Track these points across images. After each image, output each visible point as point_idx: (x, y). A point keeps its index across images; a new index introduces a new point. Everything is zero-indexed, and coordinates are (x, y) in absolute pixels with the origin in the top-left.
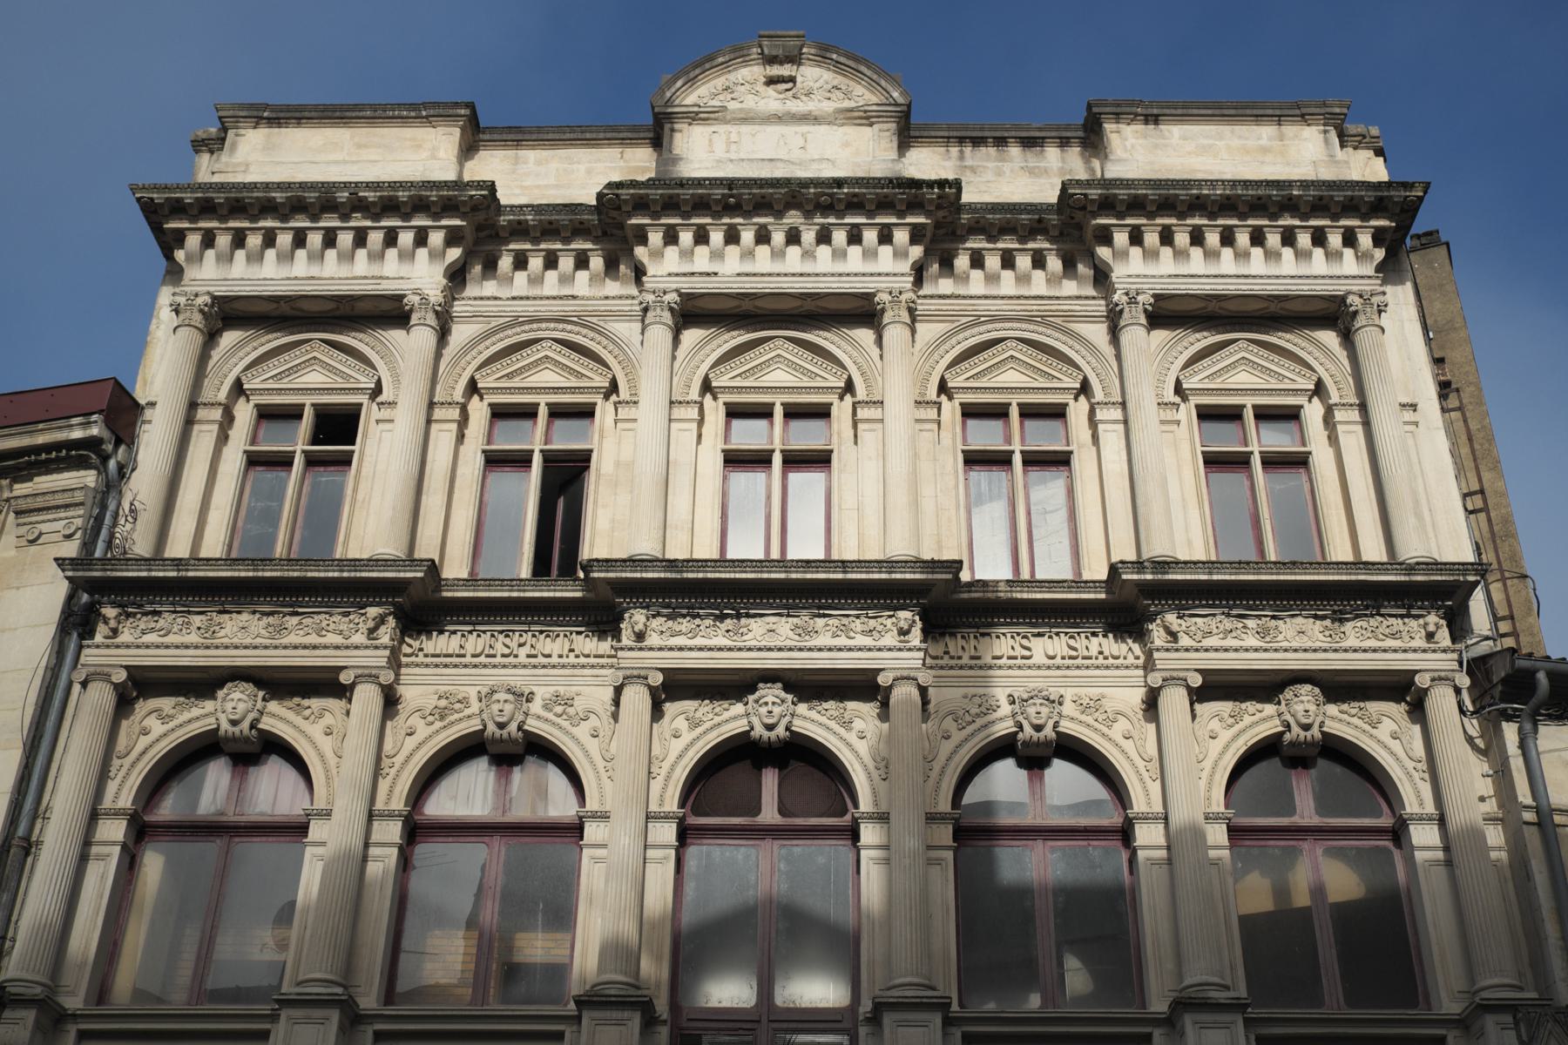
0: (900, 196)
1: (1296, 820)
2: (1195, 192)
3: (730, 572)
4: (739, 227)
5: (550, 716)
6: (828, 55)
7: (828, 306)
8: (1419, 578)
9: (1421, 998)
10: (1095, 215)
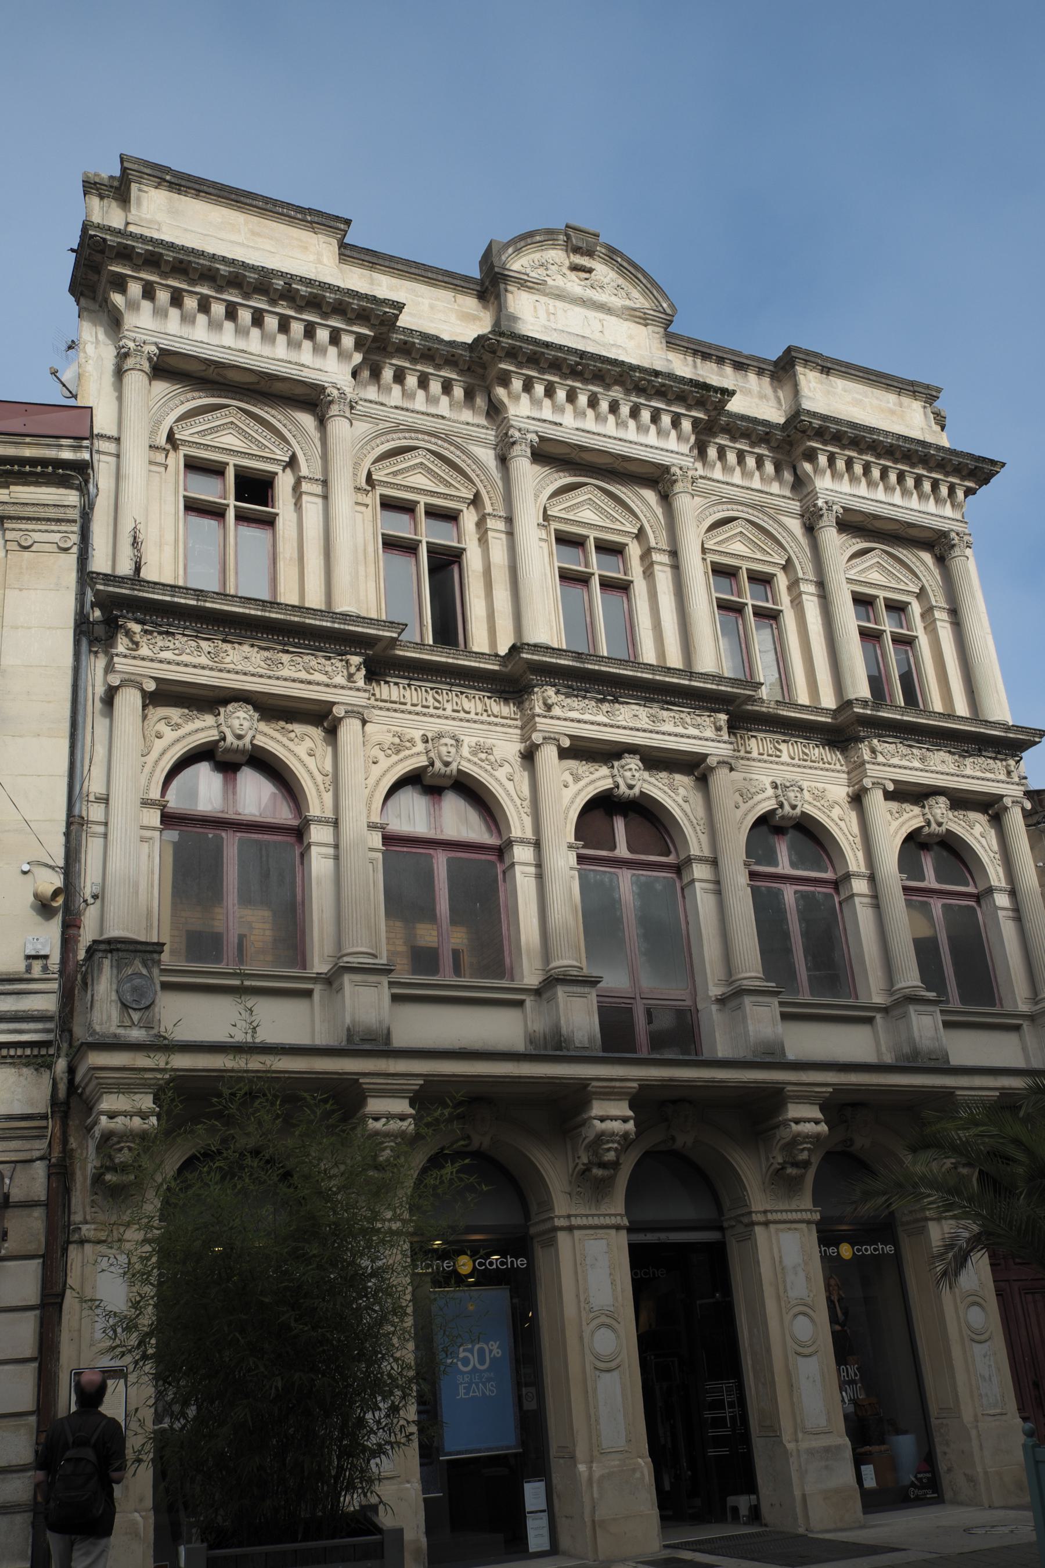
0: (695, 394)
1: (779, 870)
2: (875, 437)
3: (616, 668)
4: (578, 390)
5: (476, 760)
6: (615, 257)
7: (628, 467)
8: (1011, 735)
9: (997, 1001)
10: (810, 439)
